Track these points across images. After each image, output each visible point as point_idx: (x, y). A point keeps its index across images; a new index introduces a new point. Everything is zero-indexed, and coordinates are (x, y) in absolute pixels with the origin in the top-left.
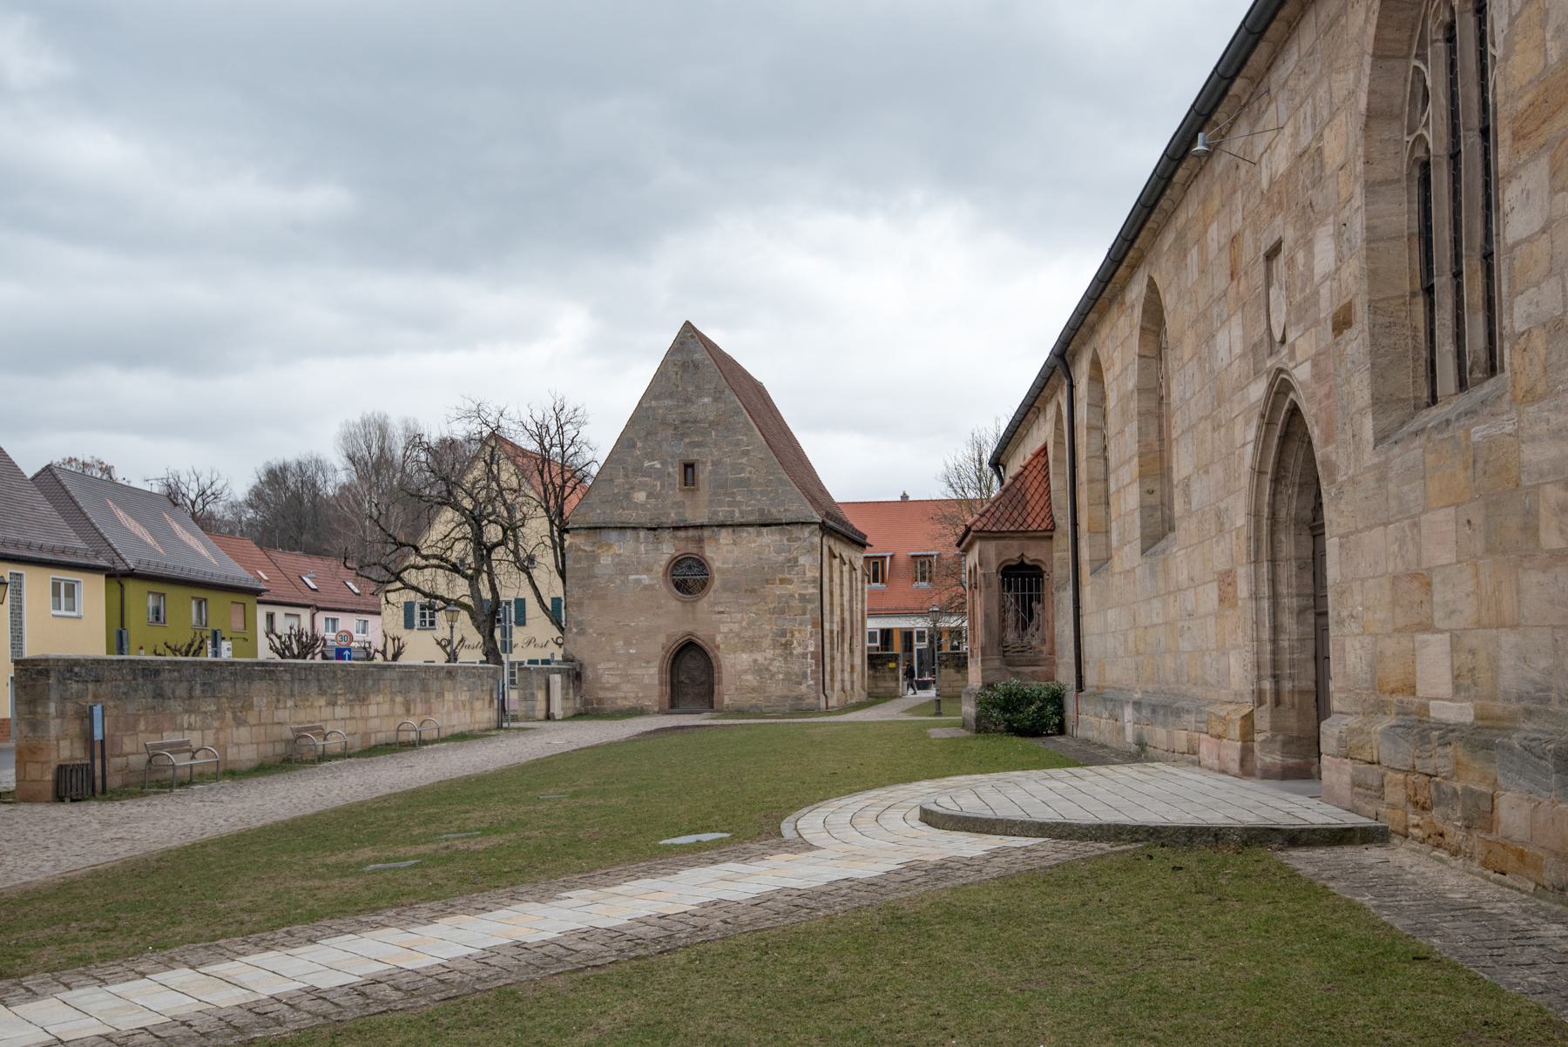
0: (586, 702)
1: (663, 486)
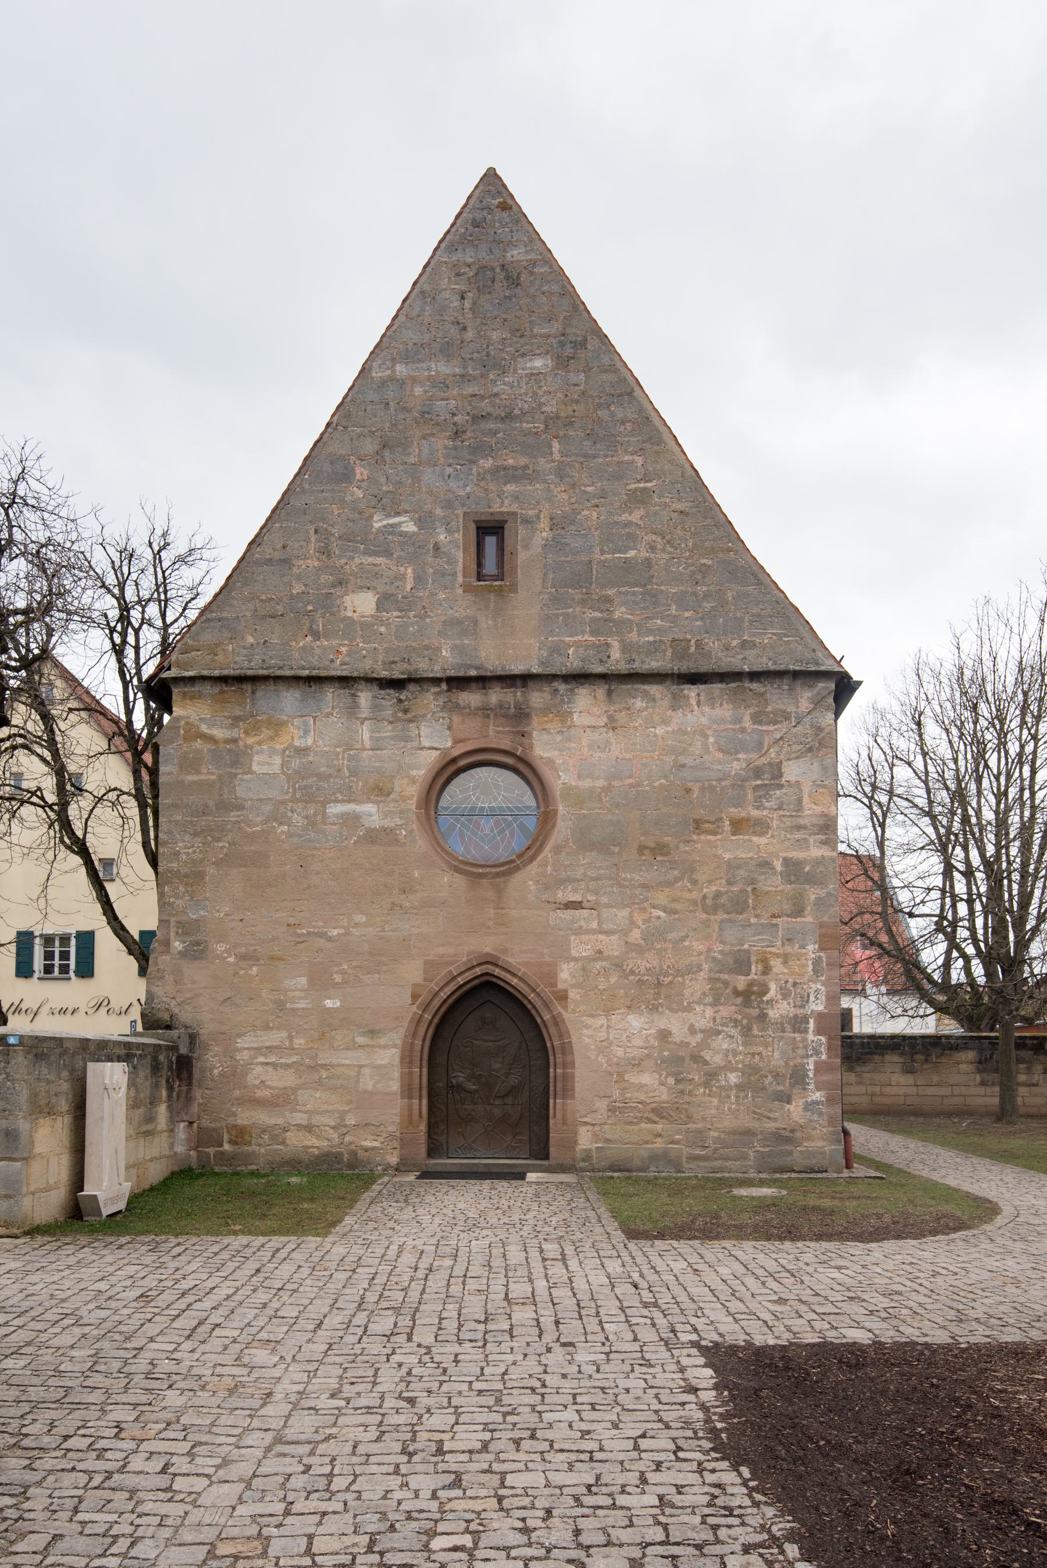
0: (203, 1138)
1: (419, 579)
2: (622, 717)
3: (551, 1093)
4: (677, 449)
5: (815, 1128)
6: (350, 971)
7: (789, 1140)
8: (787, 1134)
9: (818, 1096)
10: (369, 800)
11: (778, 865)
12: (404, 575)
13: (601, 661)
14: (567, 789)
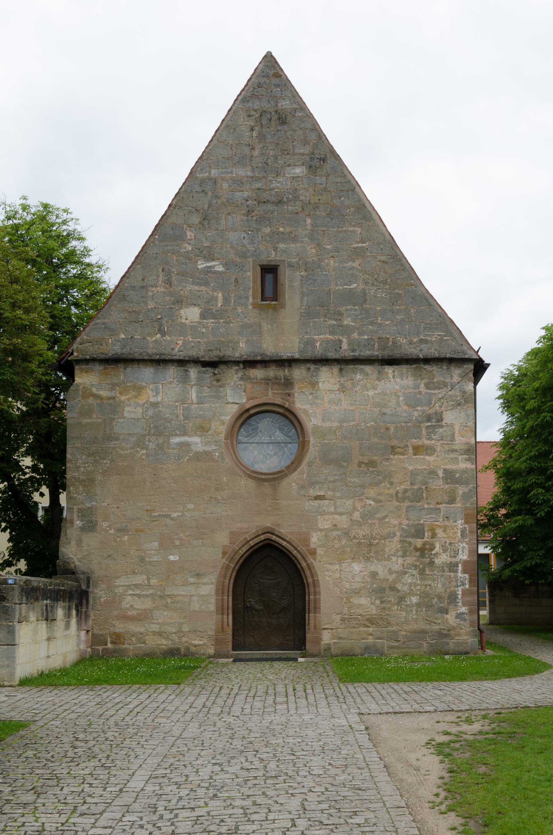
0: (96, 640)
1: (226, 300)
2: (349, 384)
3: (307, 610)
4: (380, 224)
5: (462, 629)
6: (184, 538)
7: (447, 636)
8: (446, 632)
9: (464, 609)
10: (196, 435)
11: (441, 473)
12: (217, 297)
13: (336, 350)
14: (316, 429)
